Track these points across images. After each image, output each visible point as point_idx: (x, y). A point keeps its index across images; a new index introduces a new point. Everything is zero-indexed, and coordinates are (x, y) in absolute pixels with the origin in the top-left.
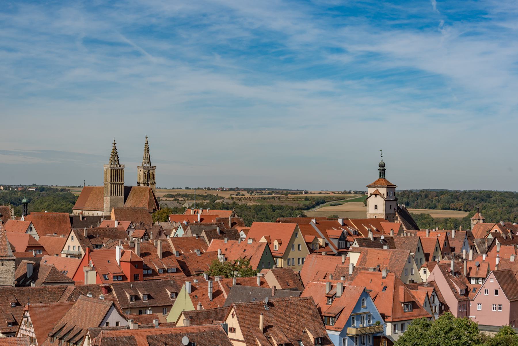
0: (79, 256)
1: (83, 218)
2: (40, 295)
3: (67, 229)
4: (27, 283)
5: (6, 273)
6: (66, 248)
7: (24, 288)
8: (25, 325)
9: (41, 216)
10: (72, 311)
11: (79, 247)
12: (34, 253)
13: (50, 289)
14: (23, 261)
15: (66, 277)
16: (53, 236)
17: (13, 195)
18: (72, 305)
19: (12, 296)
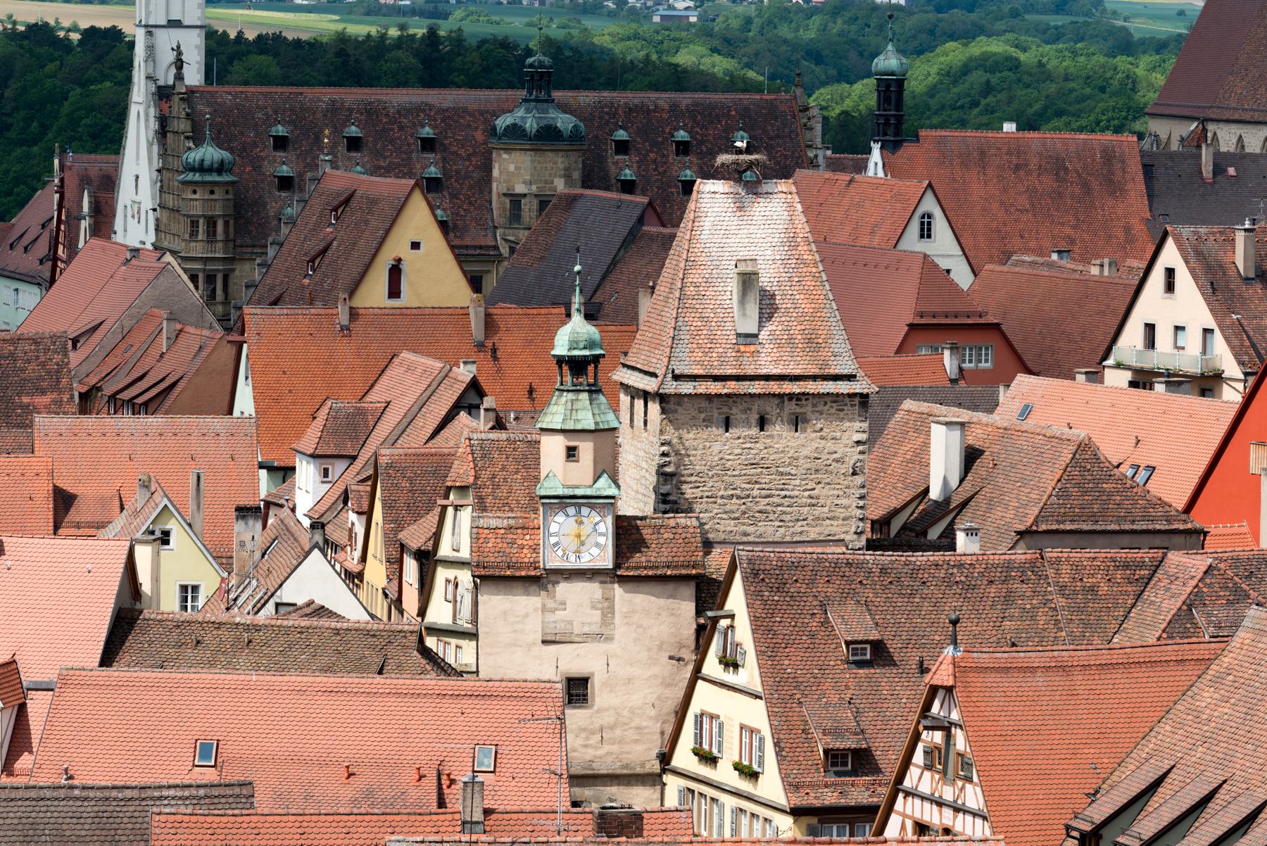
0: (1208, 383)
1: (1219, 169)
2: (1008, 599)
3: (1128, 229)
4: (934, 534)
5: (819, 469)
6: (1132, 336)
7: (920, 558)
8: (929, 767)
9: (983, 153)
10: (1206, 696)
11: (1207, 331)
12: (948, 359)
13: (1065, 569)
14: (908, 404)
15: (1154, 506)
16: (1051, 265)
17: (784, 31)
18: (1207, 662)
19: (851, 606)
